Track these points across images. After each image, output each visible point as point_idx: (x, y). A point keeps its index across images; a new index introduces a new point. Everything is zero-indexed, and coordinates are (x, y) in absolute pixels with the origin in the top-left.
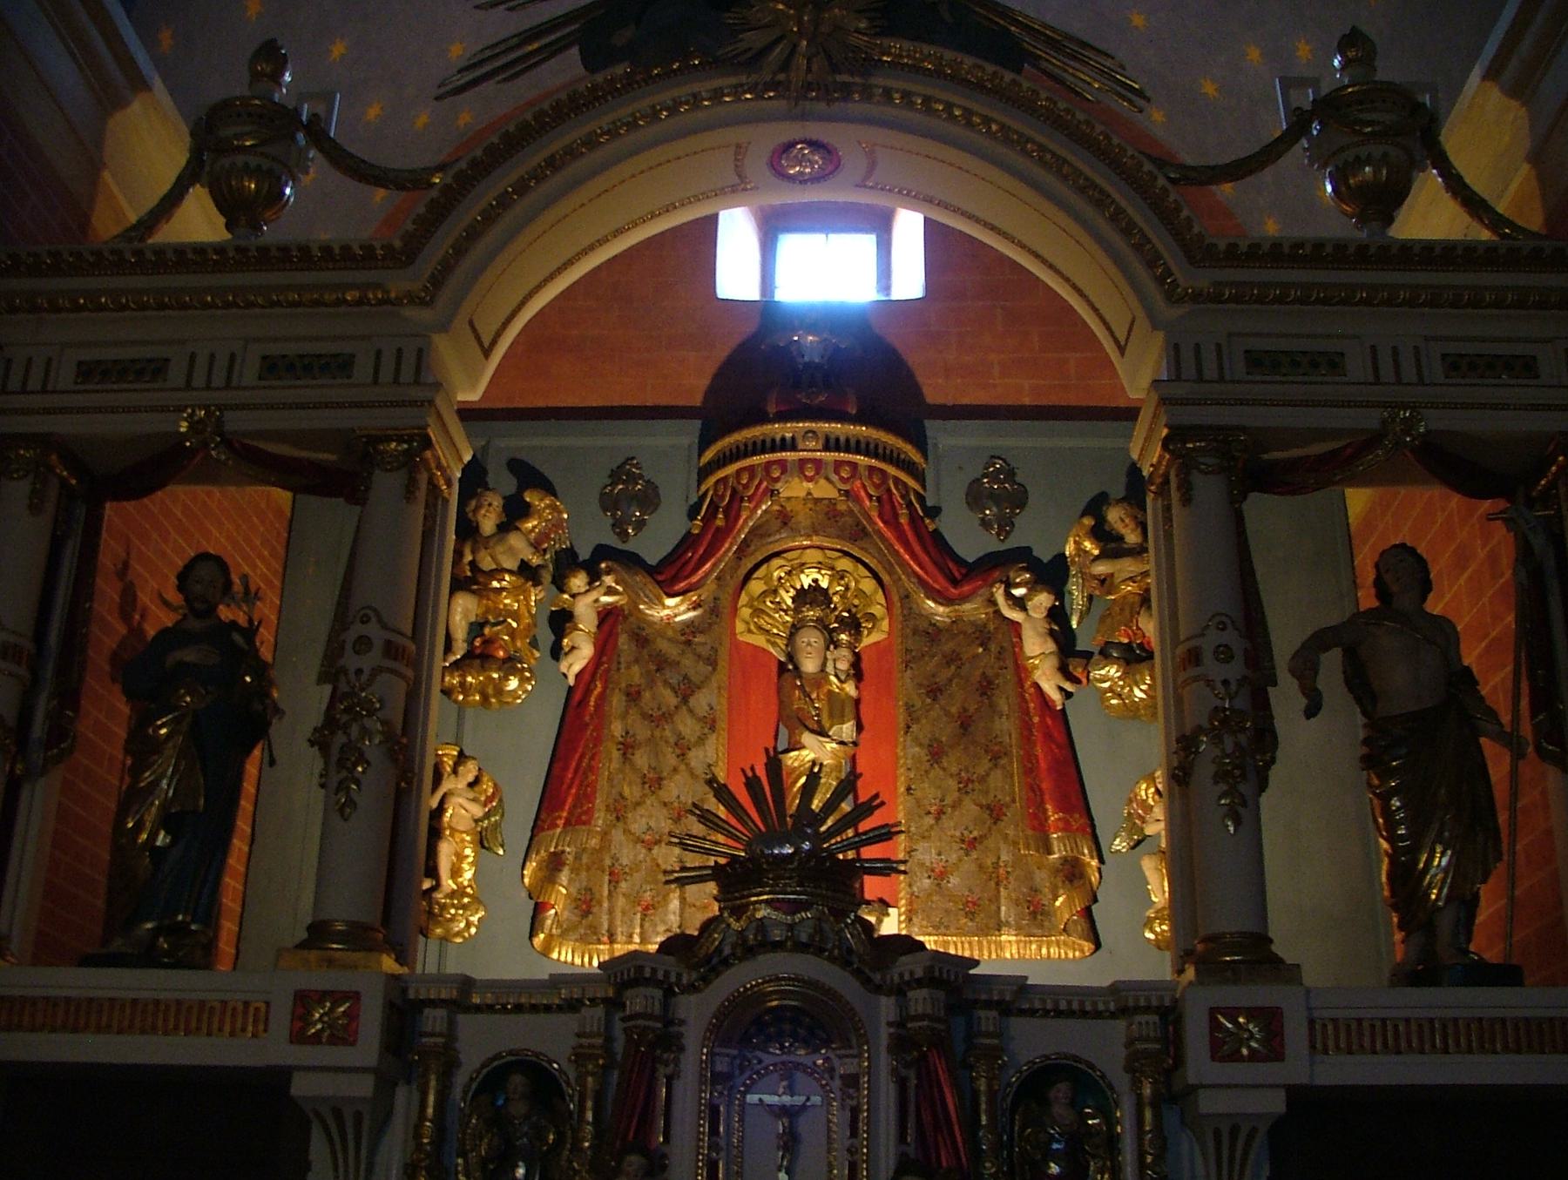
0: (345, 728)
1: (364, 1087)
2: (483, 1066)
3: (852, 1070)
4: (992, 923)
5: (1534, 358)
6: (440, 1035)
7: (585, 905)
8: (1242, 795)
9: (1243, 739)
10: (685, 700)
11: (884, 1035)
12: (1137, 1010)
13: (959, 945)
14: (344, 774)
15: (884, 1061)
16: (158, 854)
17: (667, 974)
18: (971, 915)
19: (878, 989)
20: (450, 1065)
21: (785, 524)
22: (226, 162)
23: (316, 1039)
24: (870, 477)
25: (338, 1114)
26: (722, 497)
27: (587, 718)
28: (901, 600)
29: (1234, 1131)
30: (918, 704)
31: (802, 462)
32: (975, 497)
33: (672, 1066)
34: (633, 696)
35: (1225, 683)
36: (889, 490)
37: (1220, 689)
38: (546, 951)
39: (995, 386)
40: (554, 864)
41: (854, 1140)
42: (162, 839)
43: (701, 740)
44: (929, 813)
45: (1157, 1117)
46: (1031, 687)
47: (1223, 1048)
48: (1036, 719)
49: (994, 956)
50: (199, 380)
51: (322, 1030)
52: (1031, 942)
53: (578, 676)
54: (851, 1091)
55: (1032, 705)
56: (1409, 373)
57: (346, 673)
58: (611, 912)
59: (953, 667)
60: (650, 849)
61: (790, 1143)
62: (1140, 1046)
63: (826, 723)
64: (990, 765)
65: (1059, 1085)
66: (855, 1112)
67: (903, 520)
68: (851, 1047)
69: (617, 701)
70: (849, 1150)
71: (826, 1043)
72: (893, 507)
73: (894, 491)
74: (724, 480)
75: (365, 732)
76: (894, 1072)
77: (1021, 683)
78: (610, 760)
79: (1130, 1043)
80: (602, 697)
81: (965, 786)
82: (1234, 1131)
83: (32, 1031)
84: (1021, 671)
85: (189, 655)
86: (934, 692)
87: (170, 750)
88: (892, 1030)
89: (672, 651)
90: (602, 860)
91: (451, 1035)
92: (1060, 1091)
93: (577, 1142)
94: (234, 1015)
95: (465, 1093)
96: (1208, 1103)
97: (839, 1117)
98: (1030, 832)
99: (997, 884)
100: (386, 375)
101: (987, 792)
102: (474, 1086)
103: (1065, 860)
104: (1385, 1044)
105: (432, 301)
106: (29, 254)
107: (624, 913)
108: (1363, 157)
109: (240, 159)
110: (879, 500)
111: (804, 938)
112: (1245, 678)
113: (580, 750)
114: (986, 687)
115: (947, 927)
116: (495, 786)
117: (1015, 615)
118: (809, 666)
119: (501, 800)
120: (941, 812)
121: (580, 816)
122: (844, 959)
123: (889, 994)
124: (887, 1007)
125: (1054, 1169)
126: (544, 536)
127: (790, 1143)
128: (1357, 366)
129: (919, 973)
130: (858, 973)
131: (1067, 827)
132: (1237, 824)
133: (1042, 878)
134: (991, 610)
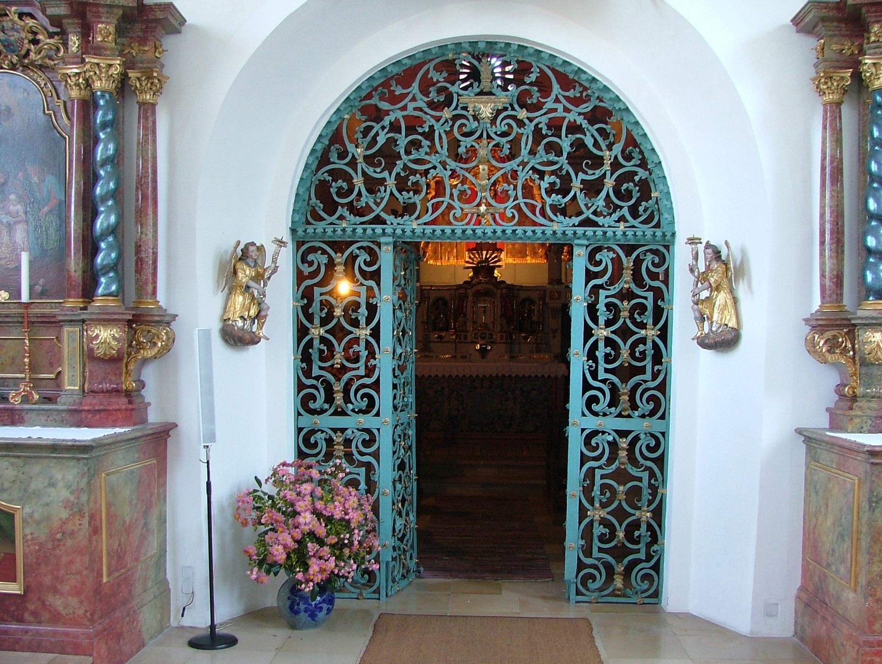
7: (435, 252)
18: (520, 254)
20: (429, 298)
45: (543, 307)
58: (441, 253)
61: (485, 312)
92: (527, 303)
93: (451, 312)
97: (492, 308)
122: (493, 285)
124: (499, 292)
125: (526, 315)
127: (485, 312)
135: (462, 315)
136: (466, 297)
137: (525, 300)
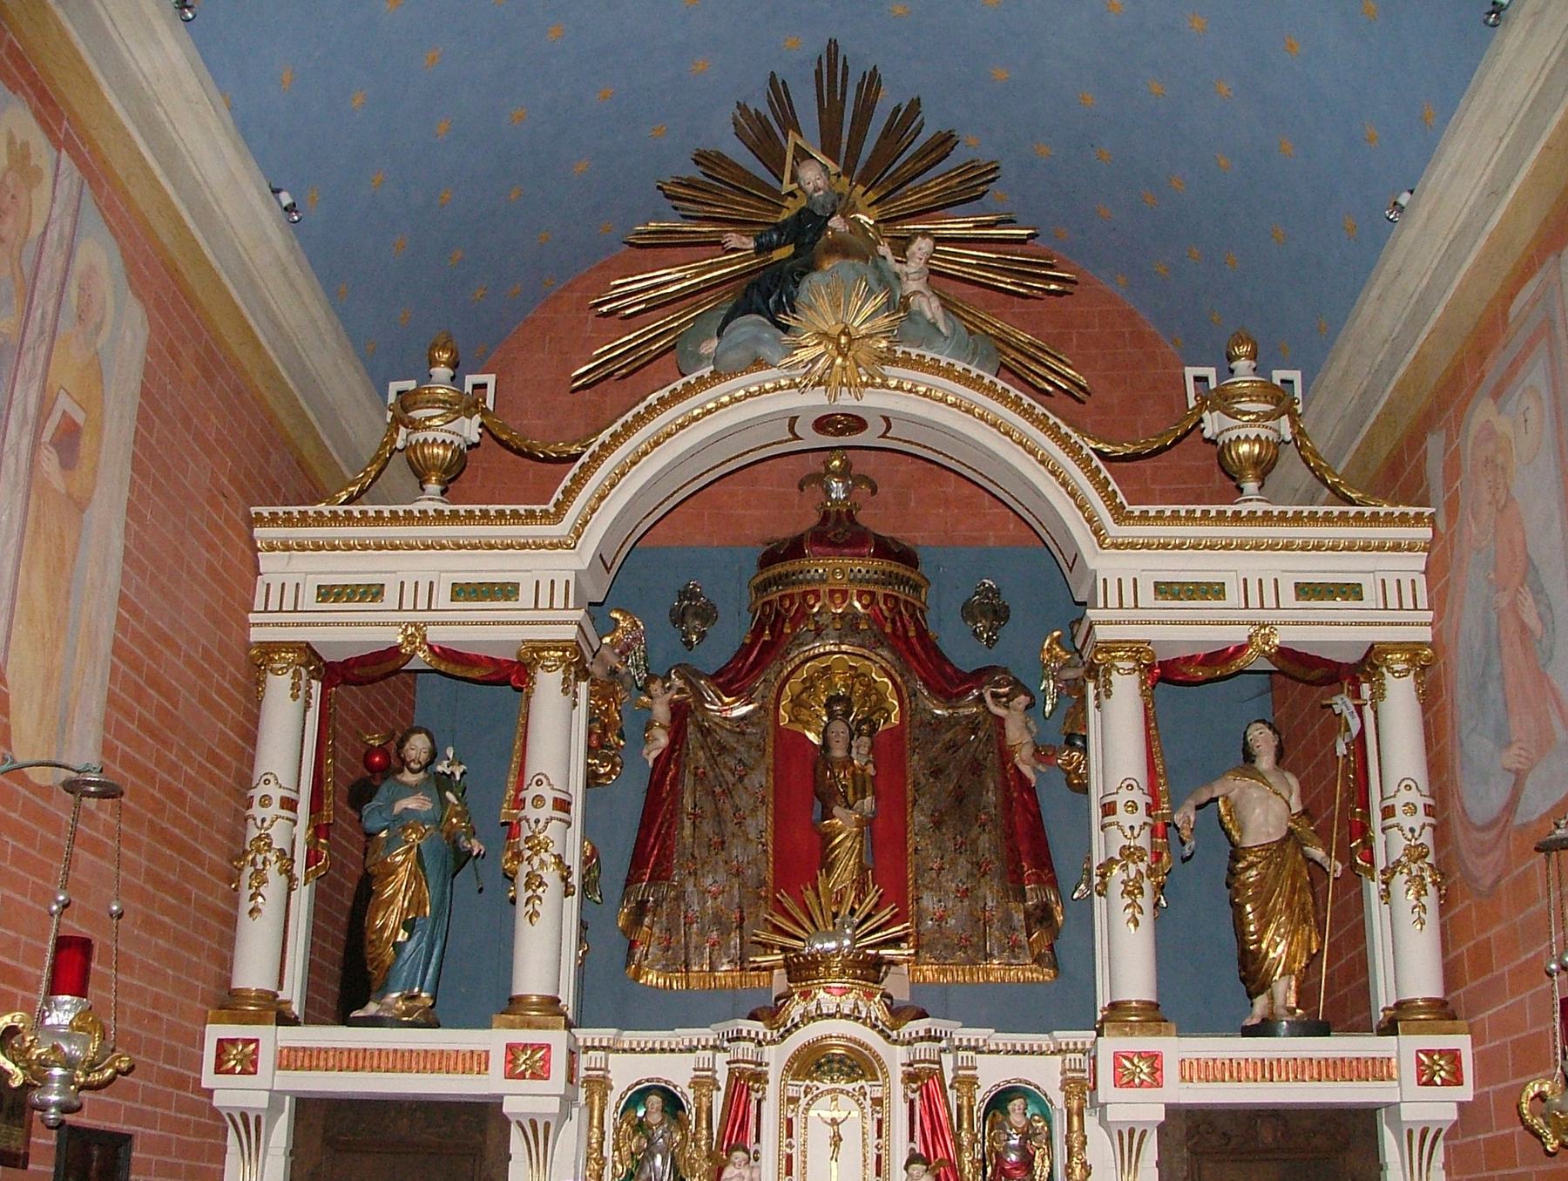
0: (529, 859)
1: (554, 1106)
2: (629, 1089)
3: (879, 1095)
4: (981, 954)
5: (1360, 585)
6: (601, 1069)
8: (1140, 907)
9: (1143, 867)
10: (741, 779)
11: (897, 1073)
12: (1067, 1051)
13: (955, 973)
14: (530, 893)
15: (898, 1089)
16: (399, 947)
17: (757, 1034)
19: (895, 1042)
21: (818, 635)
22: (420, 436)
23: (522, 1076)
24: (885, 604)
25: (534, 1124)
26: (769, 615)
27: (664, 795)
28: (910, 697)
29: (1131, 1133)
30: (923, 780)
31: (832, 593)
32: (968, 612)
33: (761, 1092)
34: (700, 778)
35: (1132, 828)
36: (900, 613)
37: (1128, 833)
38: (637, 977)
39: (985, 515)
40: (641, 909)
41: (880, 1141)
42: (402, 936)
43: (754, 810)
44: (932, 869)
46: (1011, 768)
47: (1123, 1080)
48: (1015, 795)
49: (981, 980)
50: (408, 604)
51: (526, 1070)
52: (1010, 970)
53: (656, 760)
54: (878, 1108)
55: (1012, 783)
56: (1270, 601)
57: (528, 821)
59: (950, 752)
60: (716, 898)
61: (837, 1140)
62: (1070, 1075)
63: (850, 798)
64: (980, 830)
65: (1015, 1102)
66: (880, 1122)
67: (912, 634)
68: (877, 1080)
69: (689, 780)
70: (877, 1147)
71: (862, 1076)
72: (904, 626)
73: (904, 612)
74: (770, 603)
75: (542, 862)
76: (906, 1095)
77: (1004, 764)
78: (683, 828)
79: (1063, 1072)
80: (675, 779)
81: (958, 849)
82: (1131, 1133)
83: (326, 1070)
84: (1005, 755)
85: (411, 803)
86: (937, 773)
87: (403, 874)
88: (904, 1068)
89: (731, 741)
90: (679, 907)
91: (606, 1070)
94: (464, 1059)
95: (617, 1108)
96: (1112, 1114)
97: (872, 1127)
98: (1009, 885)
99: (984, 924)
100: (544, 602)
101: (977, 851)
102: (623, 1102)
103: (1036, 907)
104: (1231, 1076)
105: (575, 547)
106: (284, 513)
107: (696, 948)
108: (1242, 437)
109: (430, 435)
110: (894, 622)
111: (847, 1011)
112: (1145, 824)
113: (659, 820)
114: (977, 768)
115: (946, 958)
116: (594, 849)
117: (1000, 711)
118: (838, 752)
119: (598, 859)
120: (941, 868)
121: (660, 874)
123: (903, 1044)
126: (629, 647)
127: (837, 1140)
128: (1233, 596)
129: (922, 1033)
130: (881, 1032)
131: (1039, 881)
132: (1137, 924)
133: (1018, 919)
134: (981, 706)
135: (739, 1155)
136: (760, 1078)
137: (1000, 1100)
